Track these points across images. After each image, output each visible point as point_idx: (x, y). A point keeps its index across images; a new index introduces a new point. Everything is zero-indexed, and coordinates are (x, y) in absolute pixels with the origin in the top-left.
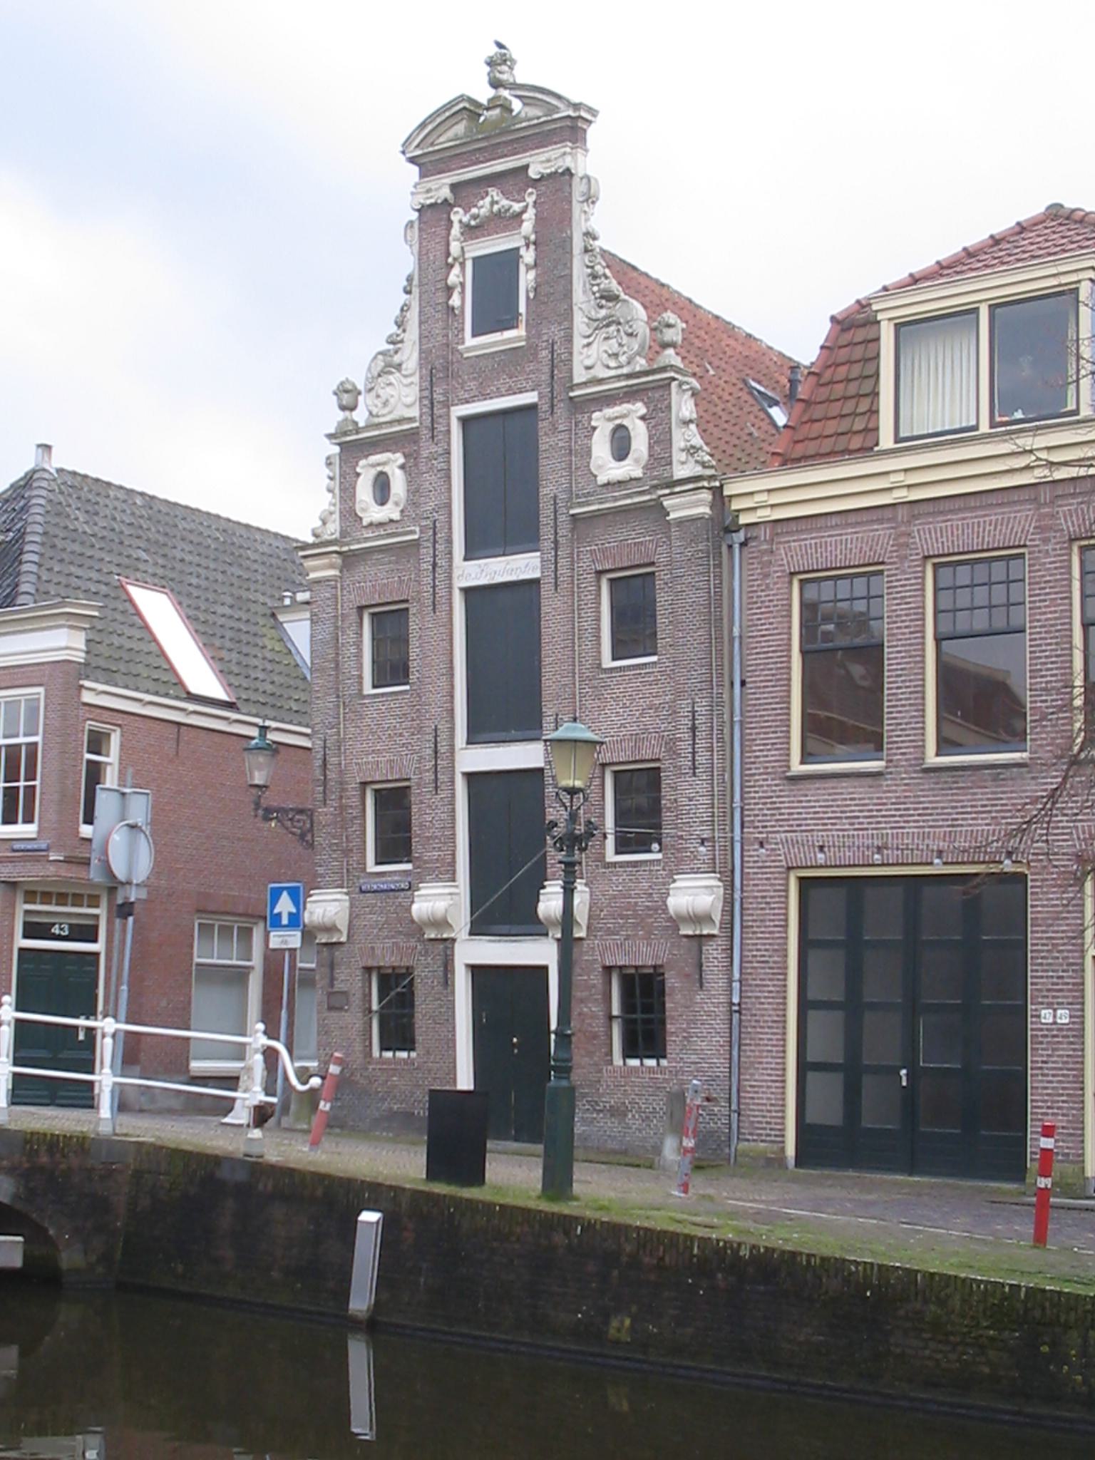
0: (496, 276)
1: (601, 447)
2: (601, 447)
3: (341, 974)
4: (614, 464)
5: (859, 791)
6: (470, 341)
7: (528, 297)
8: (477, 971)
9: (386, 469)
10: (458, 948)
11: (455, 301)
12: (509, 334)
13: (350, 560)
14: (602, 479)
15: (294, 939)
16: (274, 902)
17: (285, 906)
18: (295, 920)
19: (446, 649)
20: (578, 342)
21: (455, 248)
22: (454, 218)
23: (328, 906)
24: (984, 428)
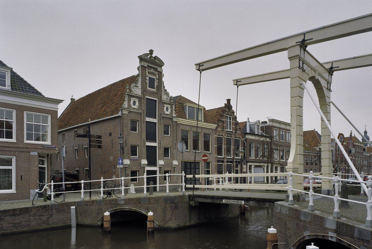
0: (152, 81)
1: (165, 110)
2: (165, 110)
3: (127, 171)
4: (166, 111)
5: (188, 153)
6: (148, 88)
7: (156, 86)
8: (147, 171)
9: (136, 101)
10: (146, 168)
11: (147, 81)
12: (153, 89)
13: (130, 112)
14: (165, 113)
15: (122, 166)
16: (119, 161)
17: (120, 161)
18: (122, 164)
19: (141, 129)
20: (163, 95)
21: (147, 74)
22: (147, 70)
23: (127, 162)
24: (203, 121)
